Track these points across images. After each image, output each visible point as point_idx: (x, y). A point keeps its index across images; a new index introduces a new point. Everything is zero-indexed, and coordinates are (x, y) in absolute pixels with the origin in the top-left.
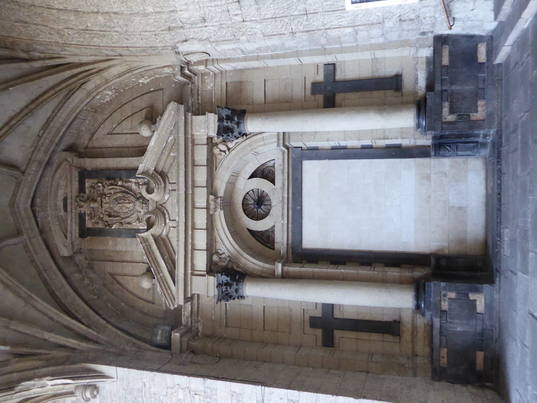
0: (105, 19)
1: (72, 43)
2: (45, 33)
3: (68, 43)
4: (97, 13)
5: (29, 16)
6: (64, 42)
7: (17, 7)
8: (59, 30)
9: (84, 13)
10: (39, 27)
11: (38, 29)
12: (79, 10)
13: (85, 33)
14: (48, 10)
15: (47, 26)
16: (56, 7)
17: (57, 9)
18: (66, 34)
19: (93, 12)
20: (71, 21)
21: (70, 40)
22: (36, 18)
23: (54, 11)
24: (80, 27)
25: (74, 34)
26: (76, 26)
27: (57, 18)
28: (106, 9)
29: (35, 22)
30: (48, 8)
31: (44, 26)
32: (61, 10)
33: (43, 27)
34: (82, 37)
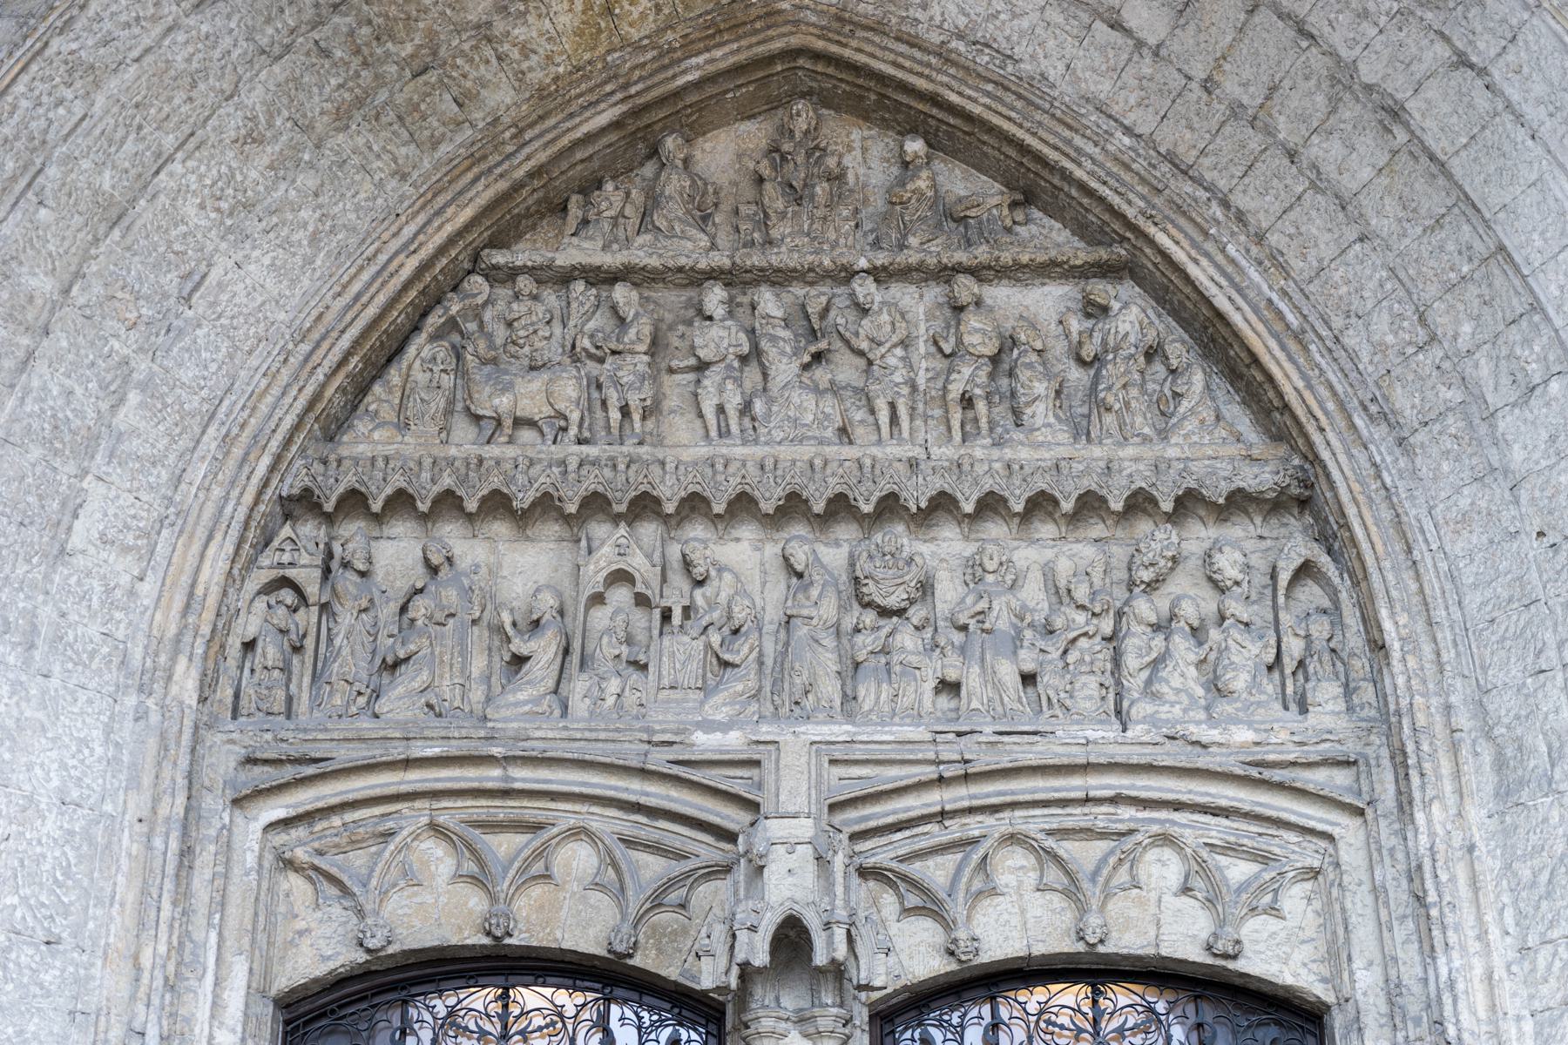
0: (31, 299)
1: (25, 78)
2: (128, 25)
3: (34, 67)
4: (66, 291)
5: (211, 40)
6: (49, 52)
7: (264, 42)
8: (97, 84)
9: (96, 241)
10: (158, 30)
11: (155, 19)
12: (116, 234)
13: (25, 168)
14: (186, 129)
15: (137, 60)
16: (177, 167)
17: (171, 159)
18: (68, 94)
19: (78, 275)
20: (99, 166)
21: (41, 87)
22: (189, 60)
23: (169, 141)
24: (53, 171)
25: (51, 122)
26: (70, 160)
27: (140, 127)
28: (61, 339)
29: (181, 37)
30: (192, 134)
31: (147, 51)
32: (157, 173)
33: (147, 41)
34: (17, 138)
